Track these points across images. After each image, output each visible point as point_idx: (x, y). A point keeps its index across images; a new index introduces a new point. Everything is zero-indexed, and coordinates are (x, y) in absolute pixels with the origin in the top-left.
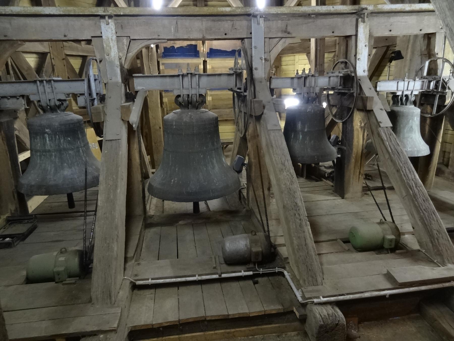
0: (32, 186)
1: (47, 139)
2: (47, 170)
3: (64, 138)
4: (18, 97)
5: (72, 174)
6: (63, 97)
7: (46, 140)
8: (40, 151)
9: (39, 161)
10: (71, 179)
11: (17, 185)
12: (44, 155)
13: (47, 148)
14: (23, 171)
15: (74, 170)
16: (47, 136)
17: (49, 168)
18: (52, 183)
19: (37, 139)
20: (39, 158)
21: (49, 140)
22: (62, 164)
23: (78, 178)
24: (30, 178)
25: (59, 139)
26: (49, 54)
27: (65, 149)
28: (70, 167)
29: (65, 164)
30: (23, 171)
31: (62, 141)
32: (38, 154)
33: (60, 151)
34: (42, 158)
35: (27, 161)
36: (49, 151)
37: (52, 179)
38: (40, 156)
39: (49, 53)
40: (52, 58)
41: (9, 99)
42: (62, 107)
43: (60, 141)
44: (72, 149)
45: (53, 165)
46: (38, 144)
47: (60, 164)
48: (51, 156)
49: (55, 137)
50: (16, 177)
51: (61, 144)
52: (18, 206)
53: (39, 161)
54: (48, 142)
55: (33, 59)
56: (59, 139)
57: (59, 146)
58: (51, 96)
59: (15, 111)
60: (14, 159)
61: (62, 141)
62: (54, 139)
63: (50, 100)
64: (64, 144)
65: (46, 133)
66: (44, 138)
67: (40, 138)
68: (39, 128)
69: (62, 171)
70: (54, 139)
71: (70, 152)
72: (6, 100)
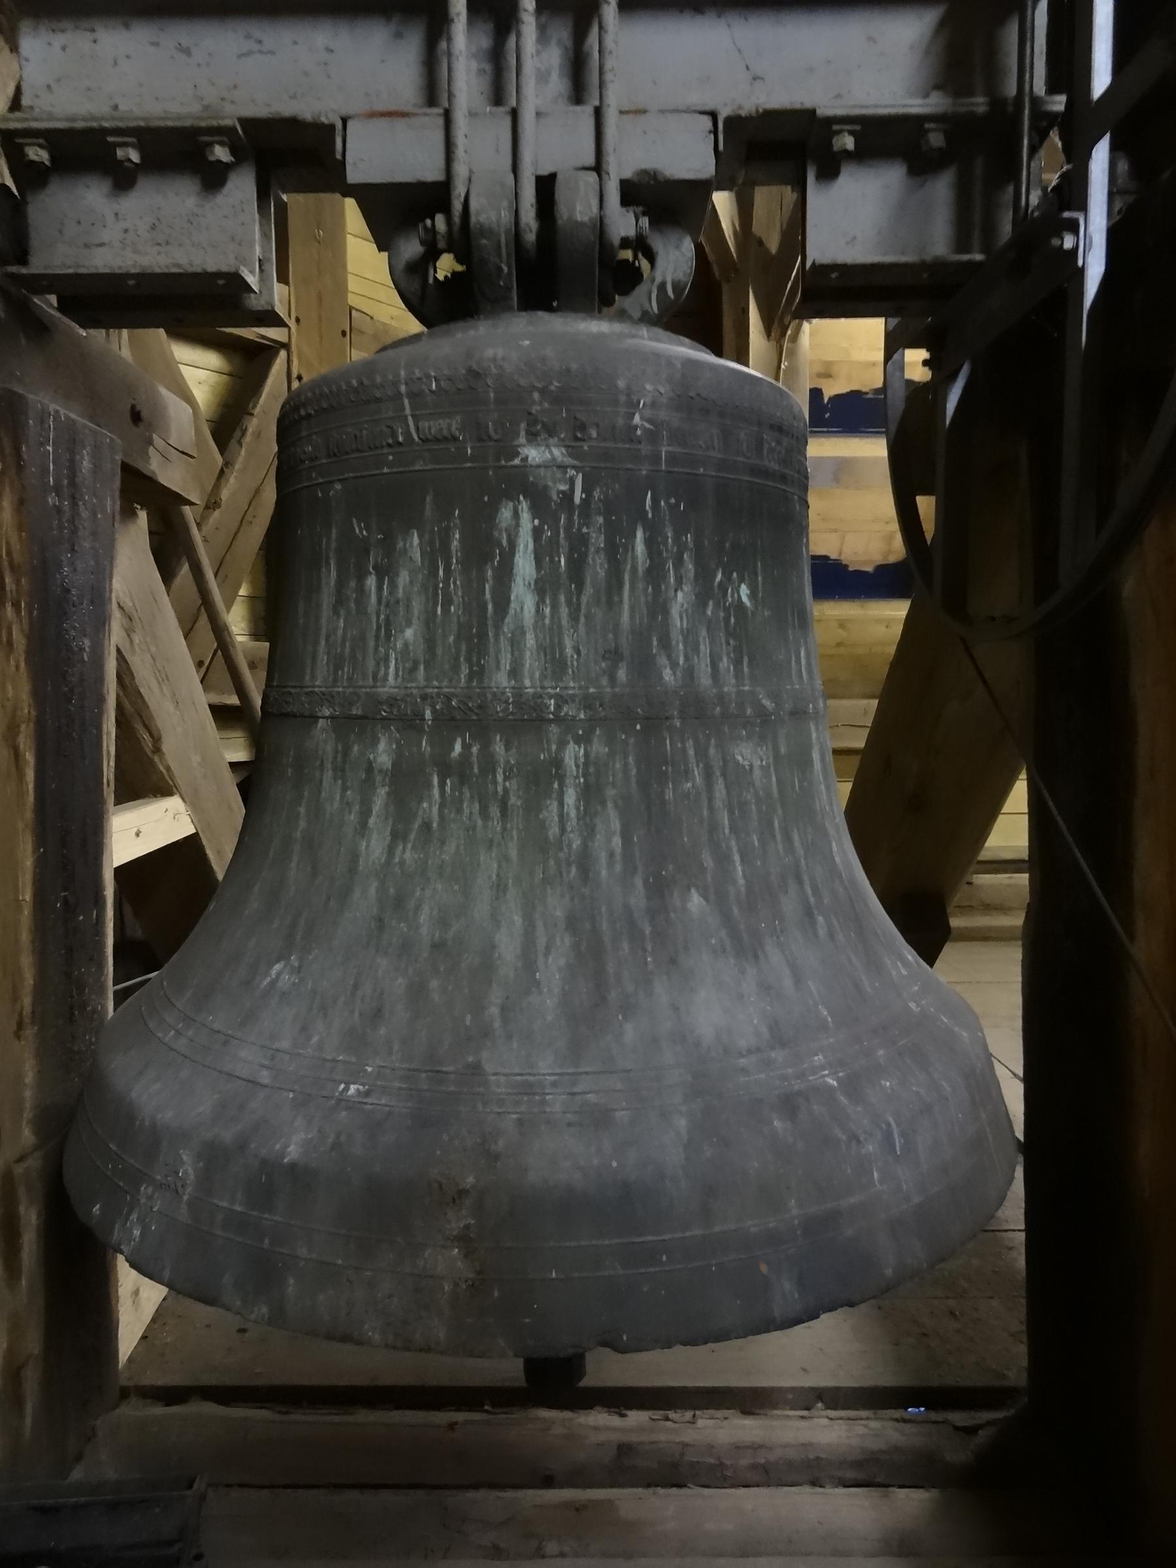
0: (275, 1183)
1: (524, 566)
2: (487, 966)
3: (703, 576)
4: (221, 153)
5: (779, 1039)
6: (689, 155)
7: (506, 572)
8: (410, 723)
9: (374, 848)
10: (789, 1105)
11: (76, 1110)
12: (460, 772)
13: (501, 680)
14: (138, 957)
15: (788, 982)
16: (520, 523)
17: (508, 946)
18: (560, 1158)
19: (385, 572)
20: (380, 798)
21: (541, 588)
22: (658, 889)
23: (853, 1086)
24: (247, 1058)
25: (655, 574)
26: (283, 353)
27: (697, 710)
28: (745, 948)
29: (696, 901)
30: (138, 957)
31: (681, 600)
32: (383, 755)
33: (647, 721)
34: (430, 807)
35: (175, 871)
36: (528, 719)
37: (556, 1103)
38: (406, 782)
39: (286, 346)
40: (295, 374)
41: (124, 180)
42: (644, 298)
43: (659, 608)
44: (763, 725)
45: (557, 906)
46: (388, 631)
47: (638, 898)
48: (542, 778)
49: (615, 553)
50: (62, 1016)
51: (665, 644)
52: (33, 1343)
53: (374, 848)
54: (523, 597)
55: (202, 374)
56: (655, 574)
57: (644, 666)
58: (556, 140)
59: (136, 417)
60: (70, 835)
61: (681, 600)
62: (597, 566)
63: (546, 185)
64: (693, 648)
65: (521, 484)
66: (487, 553)
67: (436, 552)
68: (454, 425)
69: (661, 988)
70: (597, 566)
71: (746, 754)
72: (92, 195)
